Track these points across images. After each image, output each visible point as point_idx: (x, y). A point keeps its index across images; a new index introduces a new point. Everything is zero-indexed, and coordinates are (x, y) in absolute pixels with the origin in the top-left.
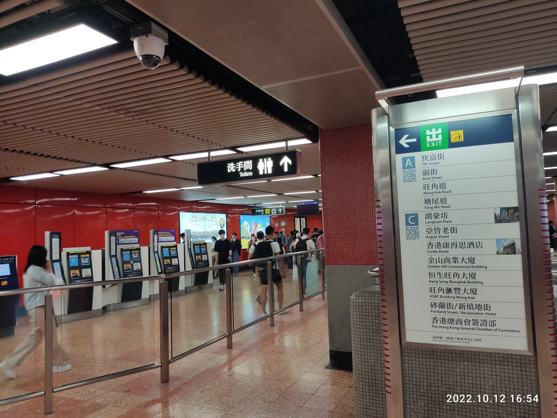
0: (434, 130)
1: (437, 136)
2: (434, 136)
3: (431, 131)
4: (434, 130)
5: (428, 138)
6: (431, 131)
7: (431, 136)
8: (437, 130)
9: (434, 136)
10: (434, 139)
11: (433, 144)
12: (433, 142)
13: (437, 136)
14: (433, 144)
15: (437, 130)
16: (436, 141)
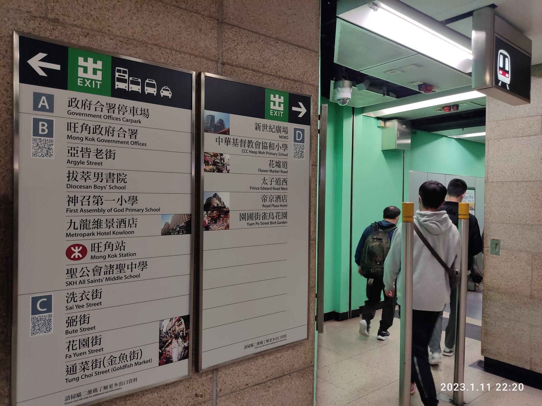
2: (90, 71)
3: (86, 60)
5: (81, 70)
6: (86, 60)
7: (85, 70)
9: (90, 71)
10: (90, 75)
11: (88, 83)
13: (95, 71)
14: (88, 83)
16: (92, 80)
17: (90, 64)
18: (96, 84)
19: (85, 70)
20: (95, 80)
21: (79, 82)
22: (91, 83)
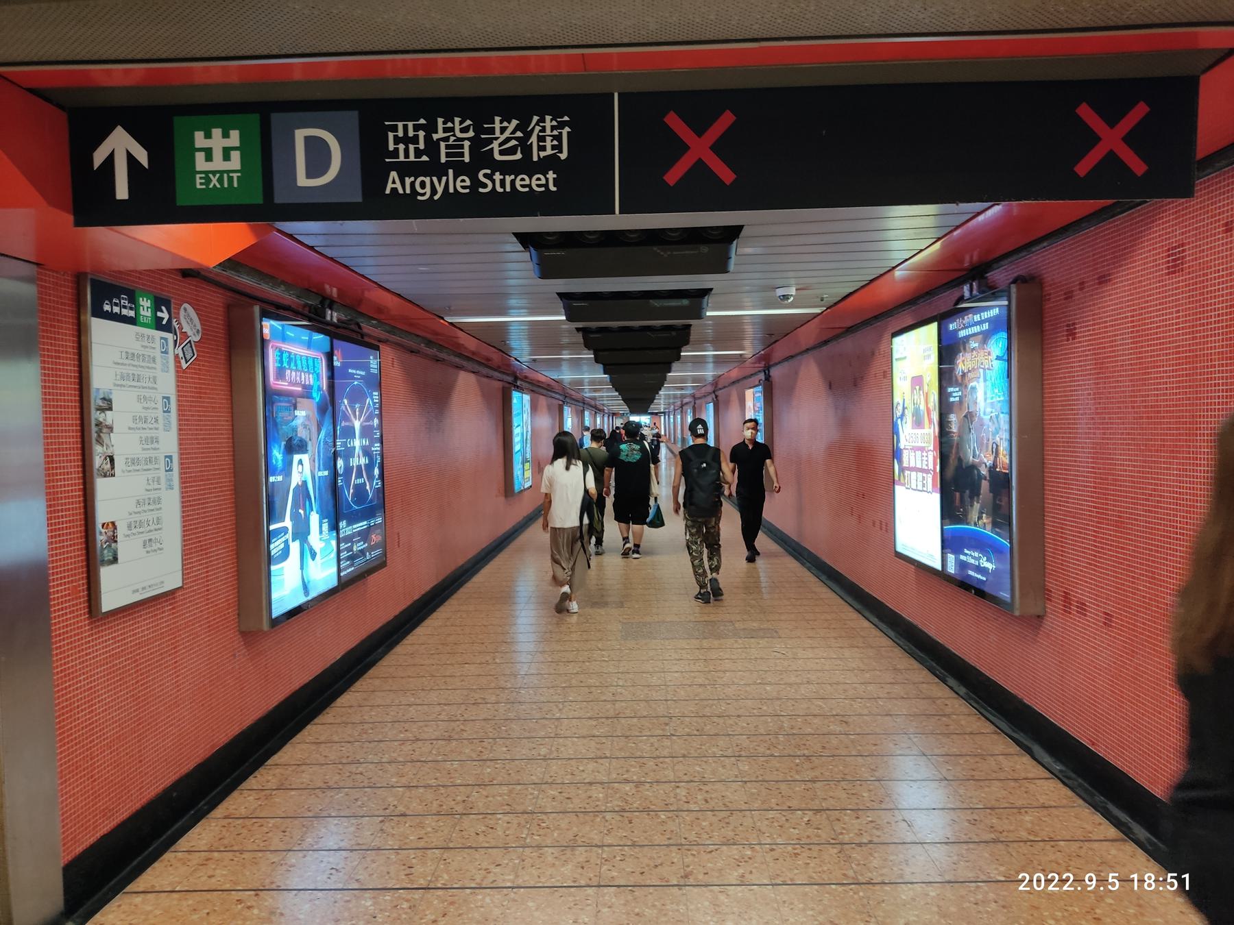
0: (217, 132)
1: (227, 157)
2: (218, 155)
3: (208, 136)
4: (217, 132)
5: (200, 157)
6: (208, 136)
8: (226, 135)
9: (218, 155)
10: (218, 164)
11: (214, 181)
12: (214, 173)
13: (227, 157)
14: (214, 181)
15: (226, 135)
16: (222, 172)
17: (217, 141)
18: (230, 179)
19: (209, 158)
20: (228, 172)
21: (198, 181)
22: (220, 180)
